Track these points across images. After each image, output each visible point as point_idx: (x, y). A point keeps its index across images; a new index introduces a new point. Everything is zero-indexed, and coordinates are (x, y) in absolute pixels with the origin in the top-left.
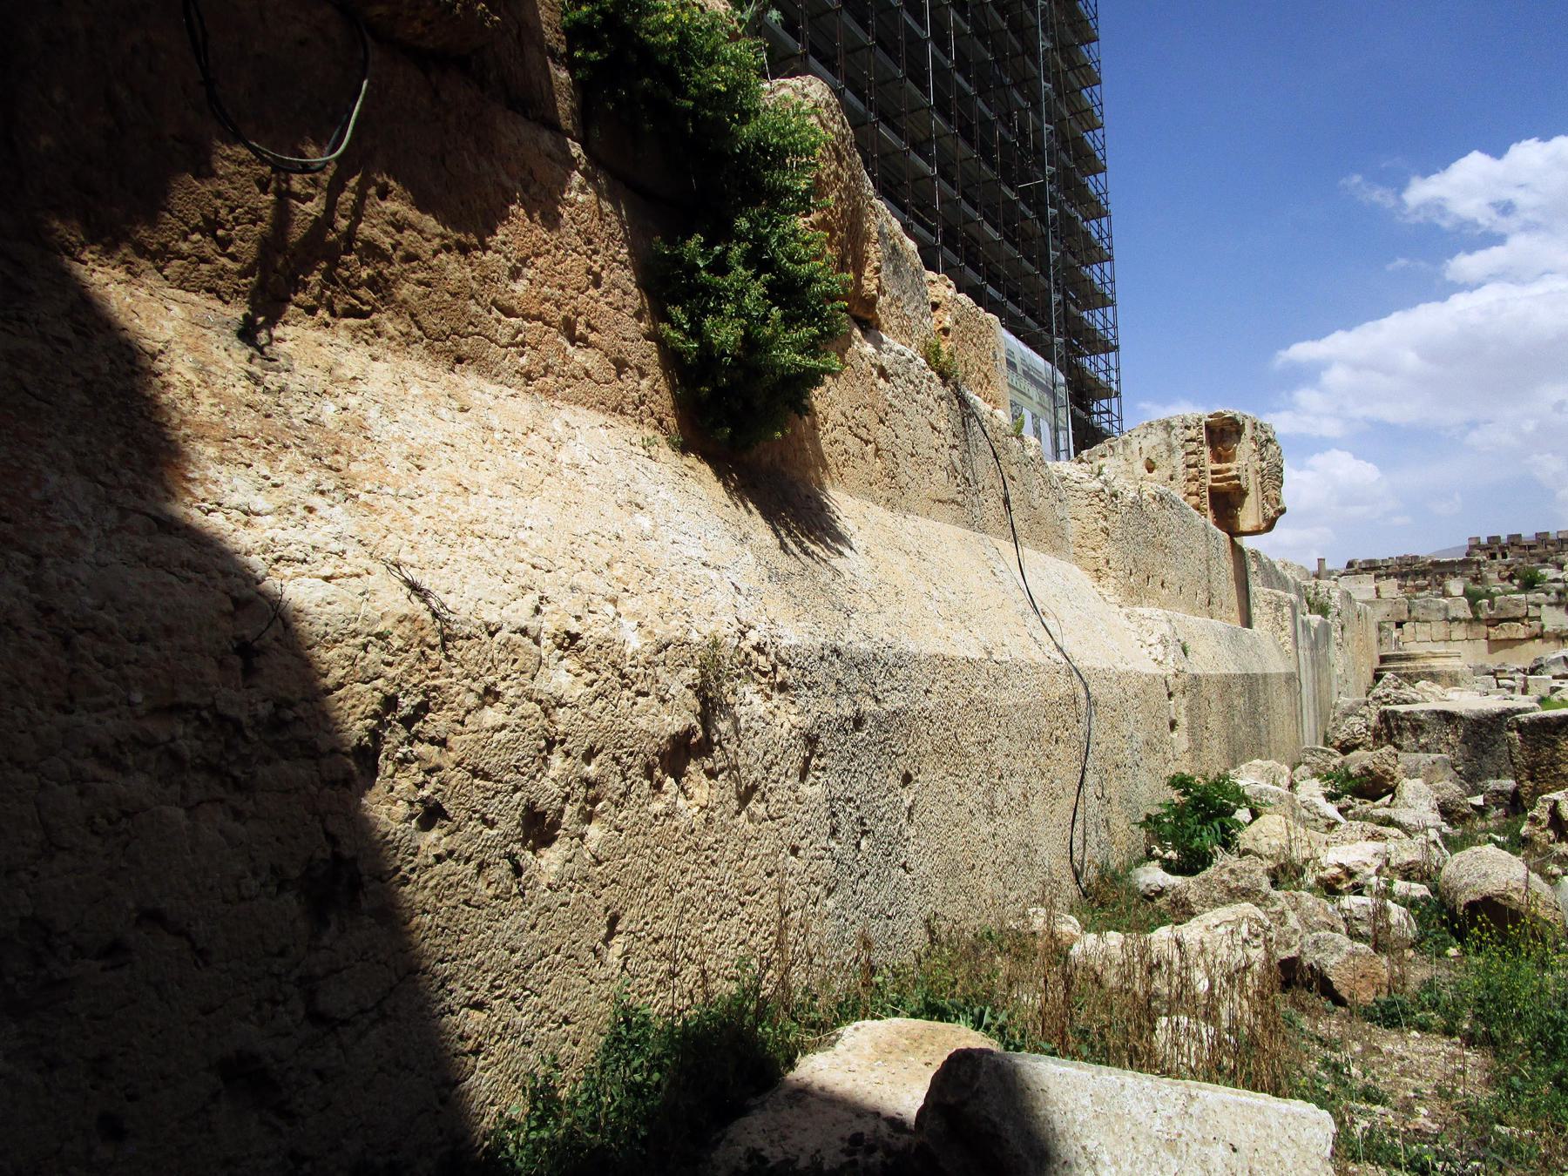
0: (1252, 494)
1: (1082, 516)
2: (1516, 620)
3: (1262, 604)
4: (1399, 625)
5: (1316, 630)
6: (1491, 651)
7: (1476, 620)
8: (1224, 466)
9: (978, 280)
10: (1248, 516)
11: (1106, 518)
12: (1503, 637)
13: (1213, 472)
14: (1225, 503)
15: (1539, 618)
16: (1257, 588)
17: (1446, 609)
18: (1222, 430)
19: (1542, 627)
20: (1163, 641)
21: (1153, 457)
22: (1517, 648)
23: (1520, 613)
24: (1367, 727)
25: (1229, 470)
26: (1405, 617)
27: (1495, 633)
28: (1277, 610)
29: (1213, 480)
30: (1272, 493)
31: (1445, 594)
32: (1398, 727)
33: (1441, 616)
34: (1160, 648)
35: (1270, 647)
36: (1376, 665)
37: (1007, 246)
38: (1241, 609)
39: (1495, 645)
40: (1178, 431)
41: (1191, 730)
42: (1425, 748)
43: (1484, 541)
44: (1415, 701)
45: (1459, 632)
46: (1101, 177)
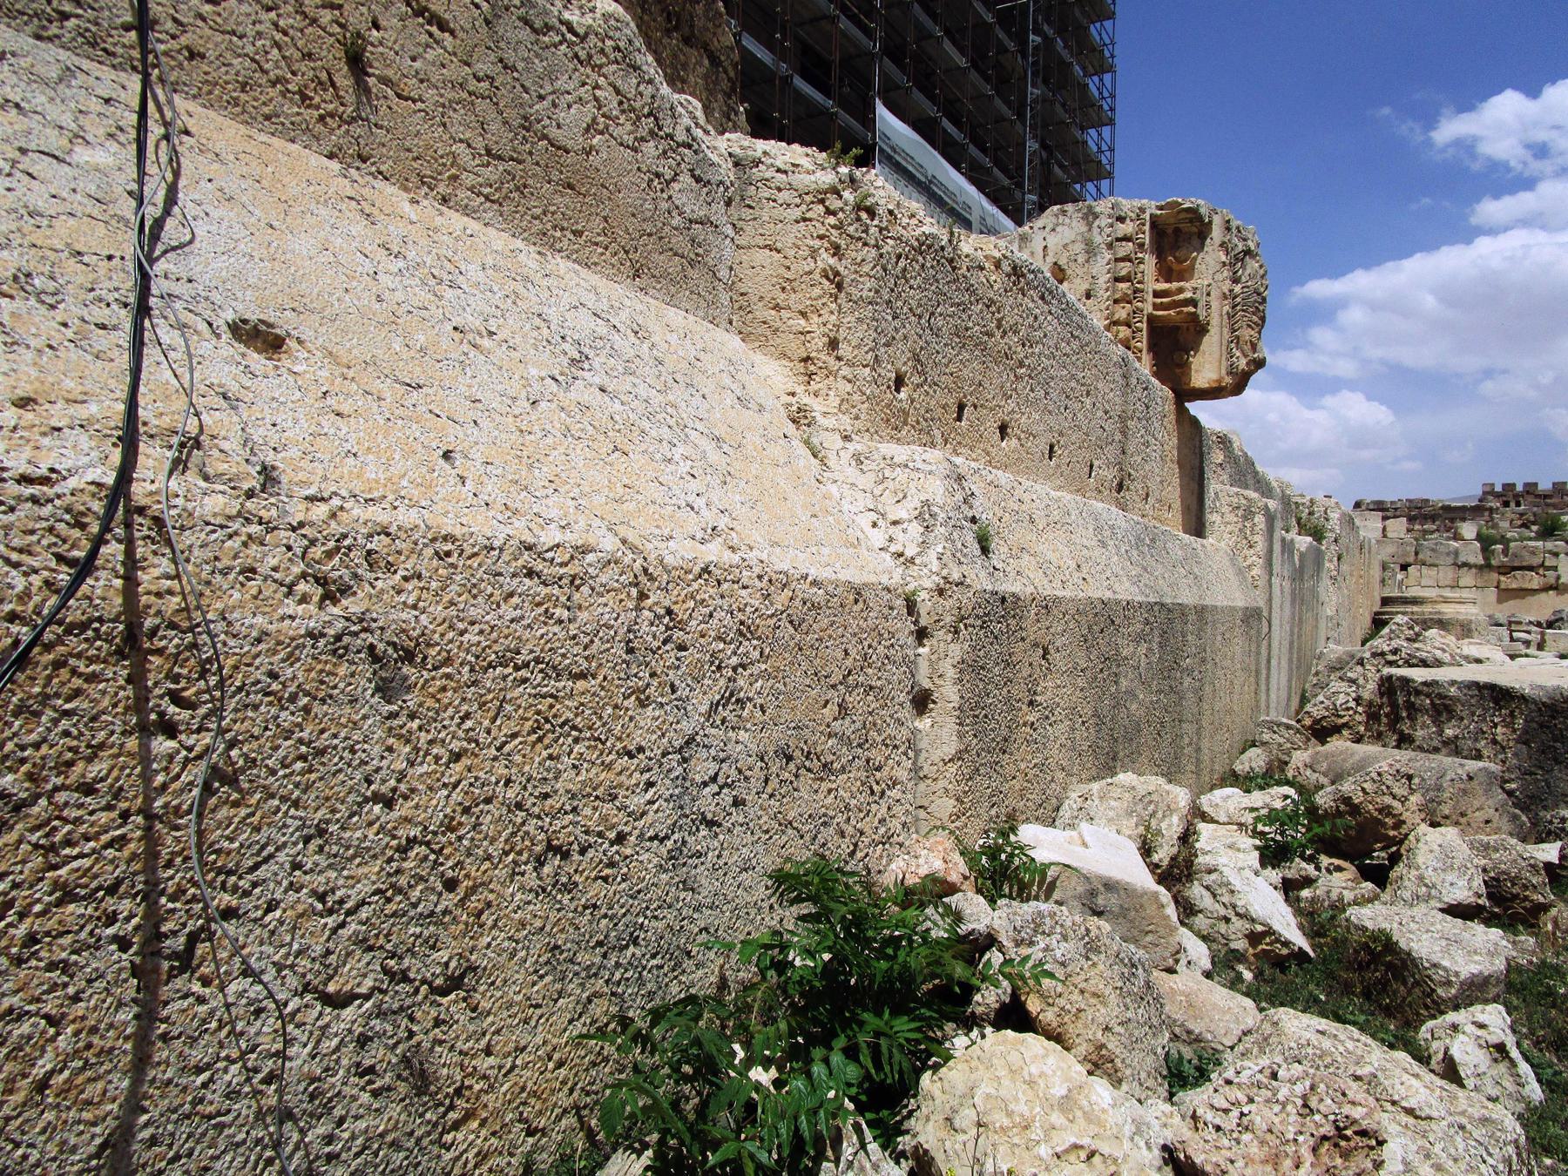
0: (1214, 330)
1: (786, 242)
2: (1531, 568)
3: (1226, 509)
4: (1404, 567)
5: (1302, 555)
6: (1500, 601)
7: (1487, 567)
8: (1175, 285)
9: (932, 111)
10: (1205, 368)
11: (836, 251)
12: (1514, 586)
13: (1156, 294)
14: (1171, 342)
15: (1555, 568)
16: (1218, 487)
17: (1456, 553)
18: (1177, 231)
19: (1558, 578)
20: (926, 516)
21: (1063, 262)
22: (1530, 599)
23: (1536, 561)
24: (1358, 700)
25: (1181, 290)
26: (1411, 559)
28: (1245, 518)
29: (1156, 306)
30: (1246, 334)
31: (1457, 537)
32: (1410, 706)
33: (1450, 560)
34: (915, 529)
35: (1221, 569)
36: (1377, 608)
37: (974, 76)
38: (1186, 509)
39: (1505, 595)
40: (1104, 221)
41: (972, 713)
42: (1453, 747)
43: (1498, 488)
44: (1439, 663)
45: (1468, 578)
46: (1108, 24)
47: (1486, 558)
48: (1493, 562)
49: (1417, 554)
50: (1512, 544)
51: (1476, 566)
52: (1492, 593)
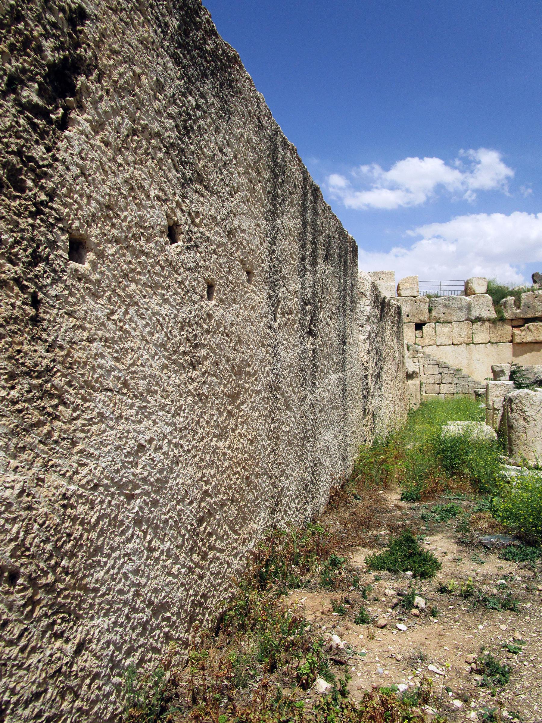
4: (419, 326)
7: (502, 319)
12: (529, 339)
17: (469, 308)
26: (425, 317)
27: (521, 335)
45: (482, 333)
47: (498, 312)
48: (507, 315)
49: (430, 311)
50: (523, 295)
51: (489, 320)
52: (507, 349)
